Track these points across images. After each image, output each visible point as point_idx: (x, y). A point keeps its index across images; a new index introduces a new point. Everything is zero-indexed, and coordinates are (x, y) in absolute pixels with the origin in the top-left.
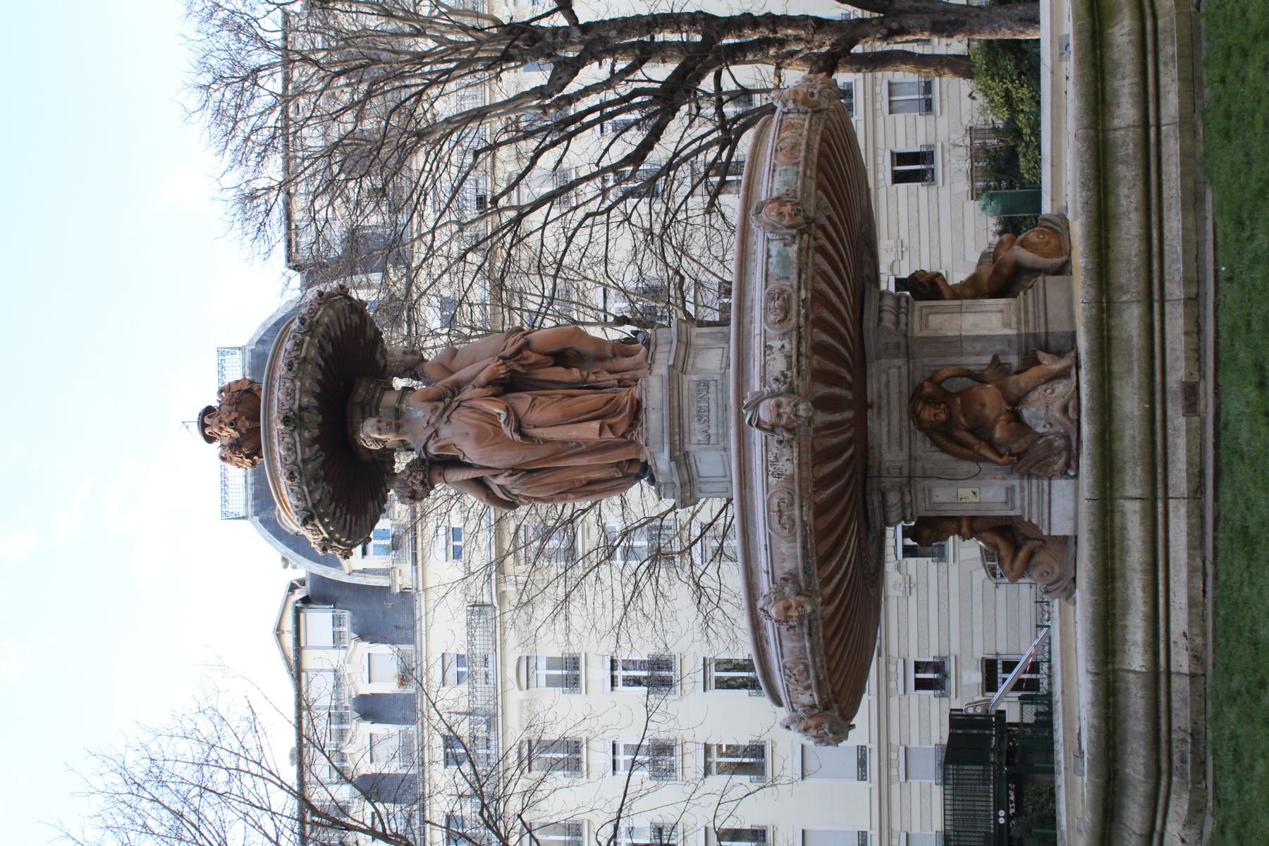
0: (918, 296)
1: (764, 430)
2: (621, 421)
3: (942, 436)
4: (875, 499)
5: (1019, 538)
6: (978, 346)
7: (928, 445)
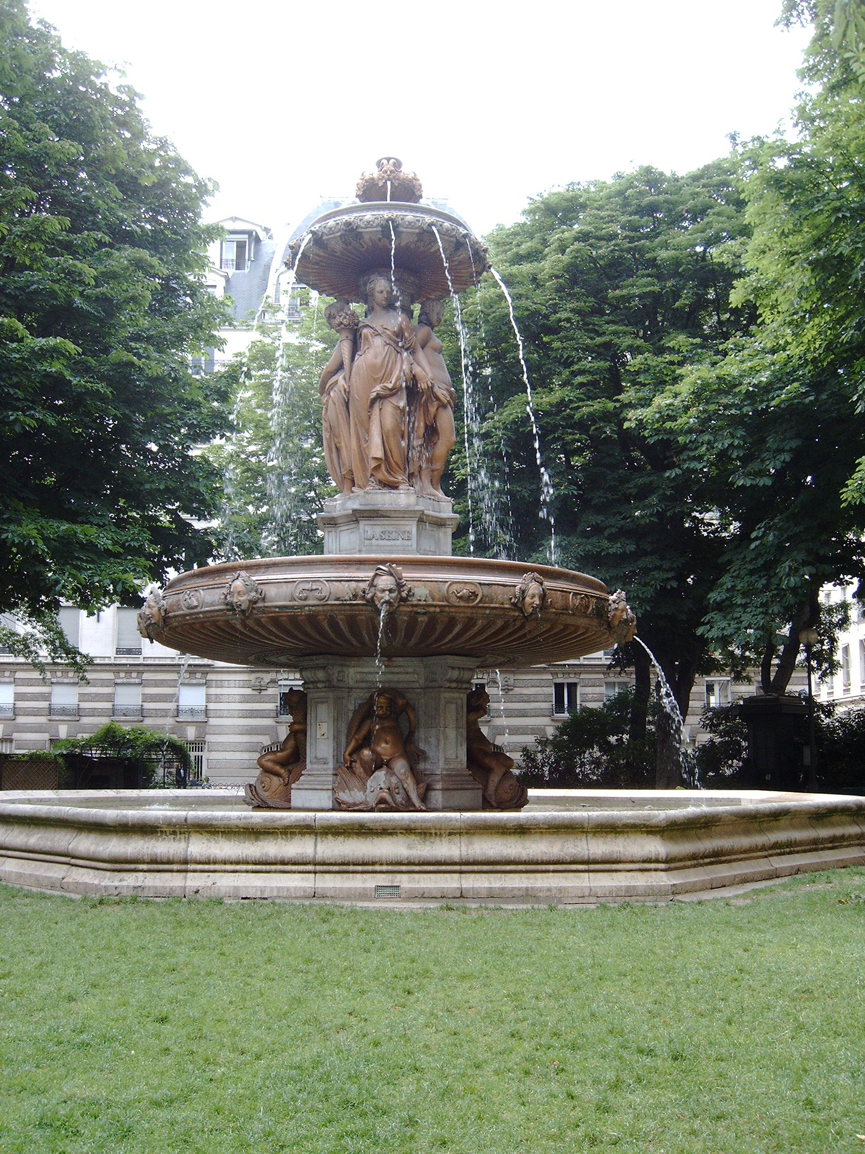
0: (470, 696)
1: (373, 580)
2: (383, 474)
3: (366, 713)
4: (321, 661)
5: (290, 767)
7: (360, 702)
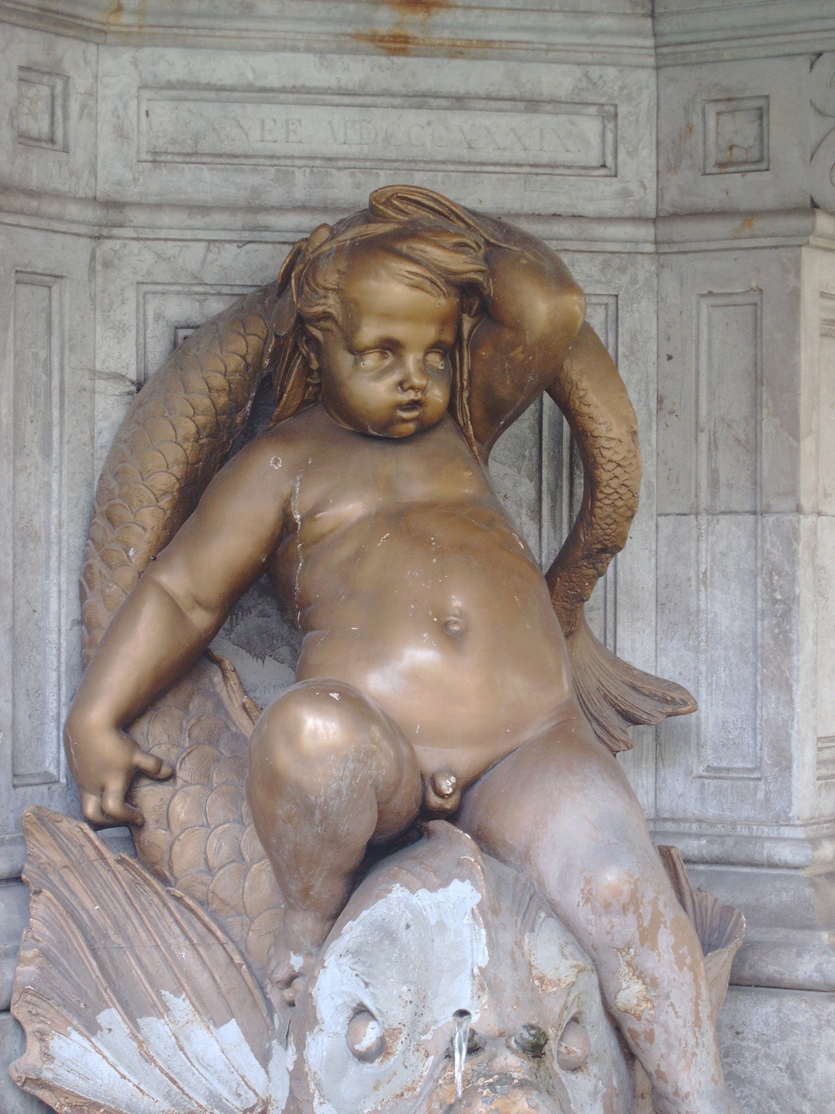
6: (725, 608)
7: (180, 309)
